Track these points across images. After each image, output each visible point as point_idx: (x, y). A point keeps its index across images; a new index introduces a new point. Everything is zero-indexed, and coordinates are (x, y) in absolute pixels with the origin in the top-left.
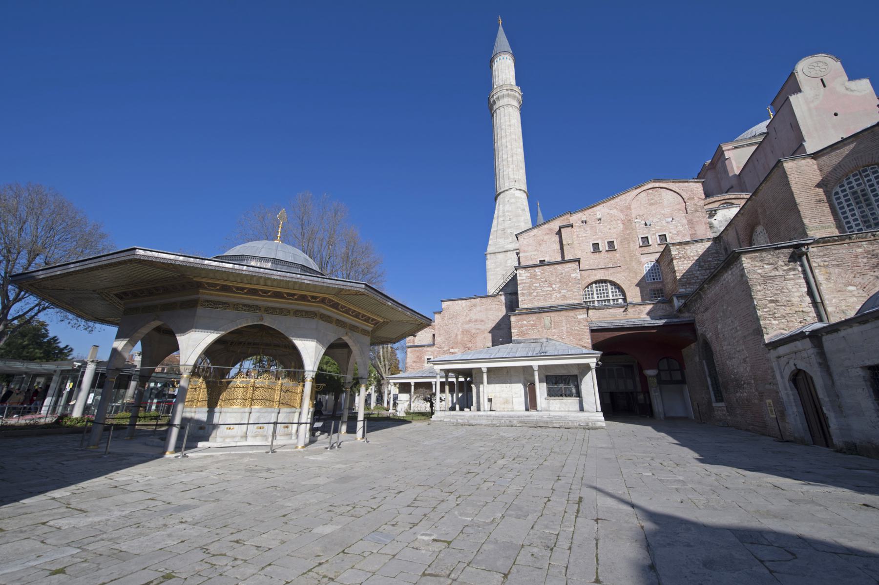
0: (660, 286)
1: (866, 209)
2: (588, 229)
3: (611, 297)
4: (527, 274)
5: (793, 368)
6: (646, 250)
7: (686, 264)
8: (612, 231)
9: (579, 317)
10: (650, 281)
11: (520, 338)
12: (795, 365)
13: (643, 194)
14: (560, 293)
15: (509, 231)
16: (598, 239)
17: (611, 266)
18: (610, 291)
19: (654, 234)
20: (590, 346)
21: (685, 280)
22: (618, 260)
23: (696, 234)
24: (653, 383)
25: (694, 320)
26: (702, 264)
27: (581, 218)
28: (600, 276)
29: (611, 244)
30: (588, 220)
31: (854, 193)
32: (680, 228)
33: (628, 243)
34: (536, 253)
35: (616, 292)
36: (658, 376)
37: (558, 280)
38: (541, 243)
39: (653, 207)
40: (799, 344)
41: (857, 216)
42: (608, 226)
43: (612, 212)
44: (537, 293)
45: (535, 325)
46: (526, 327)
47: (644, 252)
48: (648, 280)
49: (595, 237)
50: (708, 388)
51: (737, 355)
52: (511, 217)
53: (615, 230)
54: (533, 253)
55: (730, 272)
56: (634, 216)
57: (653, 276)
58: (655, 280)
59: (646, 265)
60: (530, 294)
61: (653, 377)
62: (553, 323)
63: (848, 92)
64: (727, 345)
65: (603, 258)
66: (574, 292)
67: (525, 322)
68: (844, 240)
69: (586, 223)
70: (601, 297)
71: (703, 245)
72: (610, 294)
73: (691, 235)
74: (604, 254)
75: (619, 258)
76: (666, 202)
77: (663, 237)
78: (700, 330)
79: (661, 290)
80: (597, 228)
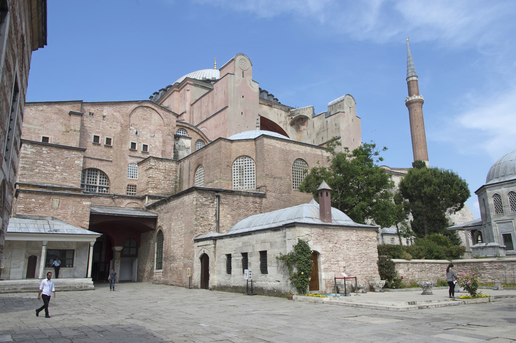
0: (135, 183)
1: (241, 176)
3: (98, 184)
4: (32, 150)
5: (203, 252)
6: (133, 154)
7: (157, 173)
9: (84, 203)
10: (129, 178)
11: (25, 214)
12: (204, 251)
14: (62, 175)
16: (99, 133)
17: (105, 159)
18: (98, 179)
19: (140, 143)
20: (88, 228)
21: (155, 185)
22: (111, 155)
23: (165, 151)
24: (118, 255)
25: (157, 217)
26: (166, 176)
27: (90, 110)
29: (109, 141)
30: (95, 112)
31: (240, 167)
32: (157, 144)
33: (122, 144)
34: (41, 128)
35: (103, 181)
36: (122, 251)
37: (62, 163)
38: (48, 120)
39: (144, 122)
40: (208, 242)
41: (238, 179)
42: (110, 125)
43: (115, 114)
44: (39, 170)
45: (43, 204)
46: (33, 205)
47: (130, 154)
48: (128, 177)
49: (97, 130)
50: (153, 262)
51: (178, 243)
53: (115, 130)
54: (38, 127)
55: (188, 196)
56: (131, 123)
57: (132, 174)
58: (133, 178)
59: (130, 165)
60: (32, 170)
61: (119, 251)
62: (60, 205)
63: (251, 87)
64: (174, 236)
66: (74, 177)
67: (33, 200)
68: (232, 193)
69: (93, 115)
70: (90, 182)
71: (170, 164)
72: (98, 182)
73: (162, 151)
75: (112, 154)
76: (153, 121)
77: (145, 147)
78: (159, 223)
80: (101, 123)
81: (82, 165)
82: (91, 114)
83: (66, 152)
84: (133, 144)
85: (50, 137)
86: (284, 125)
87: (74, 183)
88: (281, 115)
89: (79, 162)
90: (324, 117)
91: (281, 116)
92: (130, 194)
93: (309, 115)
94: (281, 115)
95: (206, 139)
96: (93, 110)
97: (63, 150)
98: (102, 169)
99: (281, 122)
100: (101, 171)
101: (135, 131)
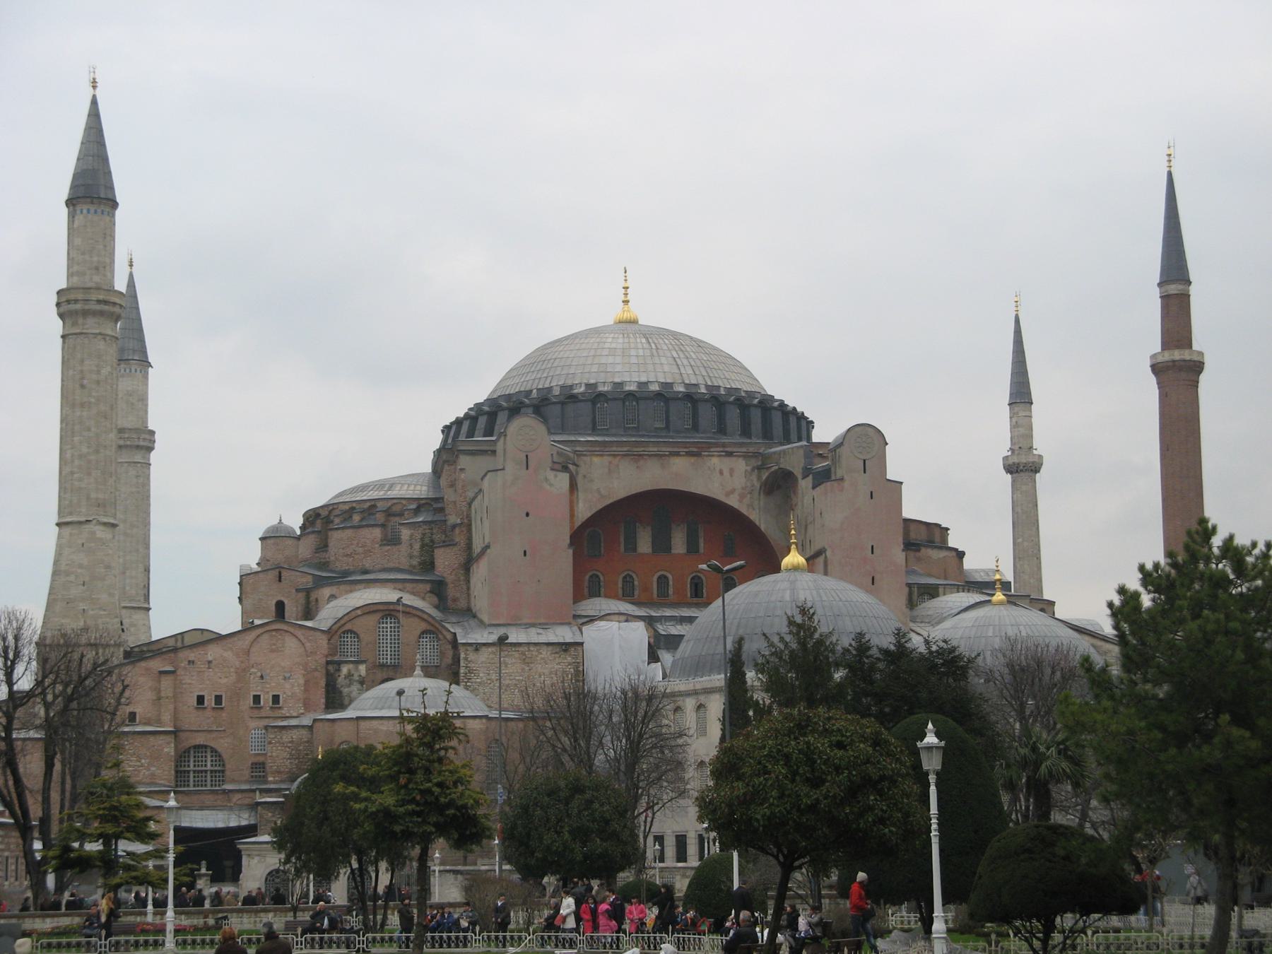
2: (195, 673)
8: (224, 681)
10: (253, 752)
13: (266, 636)
15: (82, 606)
17: (215, 728)
18: (209, 759)
22: (224, 720)
28: (200, 739)
29: (218, 699)
32: (296, 690)
42: (219, 674)
52: (87, 579)
59: (253, 732)
65: (205, 719)
72: (209, 764)
74: (209, 713)
77: (276, 699)
79: (264, 764)
81: (173, 754)
82: (191, 662)
83: (152, 738)
84: (257, 699)
85: (137, 710)
86: (742, 497)
87: (165, 779)
88: (732, 471)
89: (170, 750)
90: (811, 486)
91: (731, 476)
92: (256, 776)
93: (798, 472)
94: (732, 471)
95: (440, 628)
96: (192, 655)
97: (148, 736)
98: (212, 745)
99: (733, 491)
100: (212, 748)
101: (259, 674)
